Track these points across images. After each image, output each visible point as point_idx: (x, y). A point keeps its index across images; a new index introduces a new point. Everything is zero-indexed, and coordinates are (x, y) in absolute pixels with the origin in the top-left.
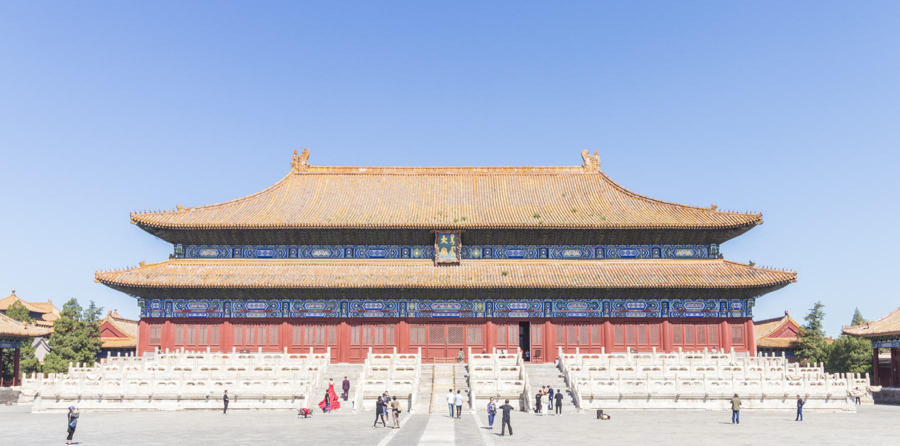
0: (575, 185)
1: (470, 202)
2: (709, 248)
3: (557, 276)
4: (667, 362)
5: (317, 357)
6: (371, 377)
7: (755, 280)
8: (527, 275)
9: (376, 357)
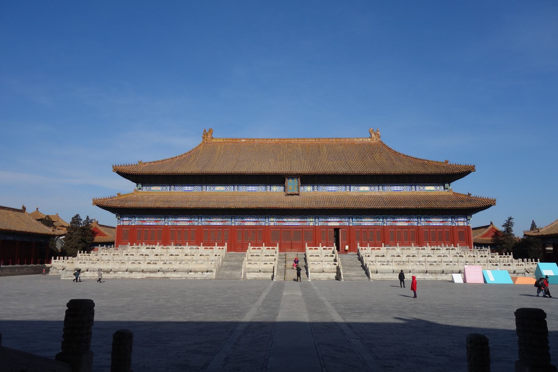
0: (366, 149)
1: (305, 159)
2: (444, 186)
3: (356, 202)
4: (420, 252)
5: (219, 248)
6: (250, 260)
7: (471, 204)
8: (339, 201)
9: (253, 249)
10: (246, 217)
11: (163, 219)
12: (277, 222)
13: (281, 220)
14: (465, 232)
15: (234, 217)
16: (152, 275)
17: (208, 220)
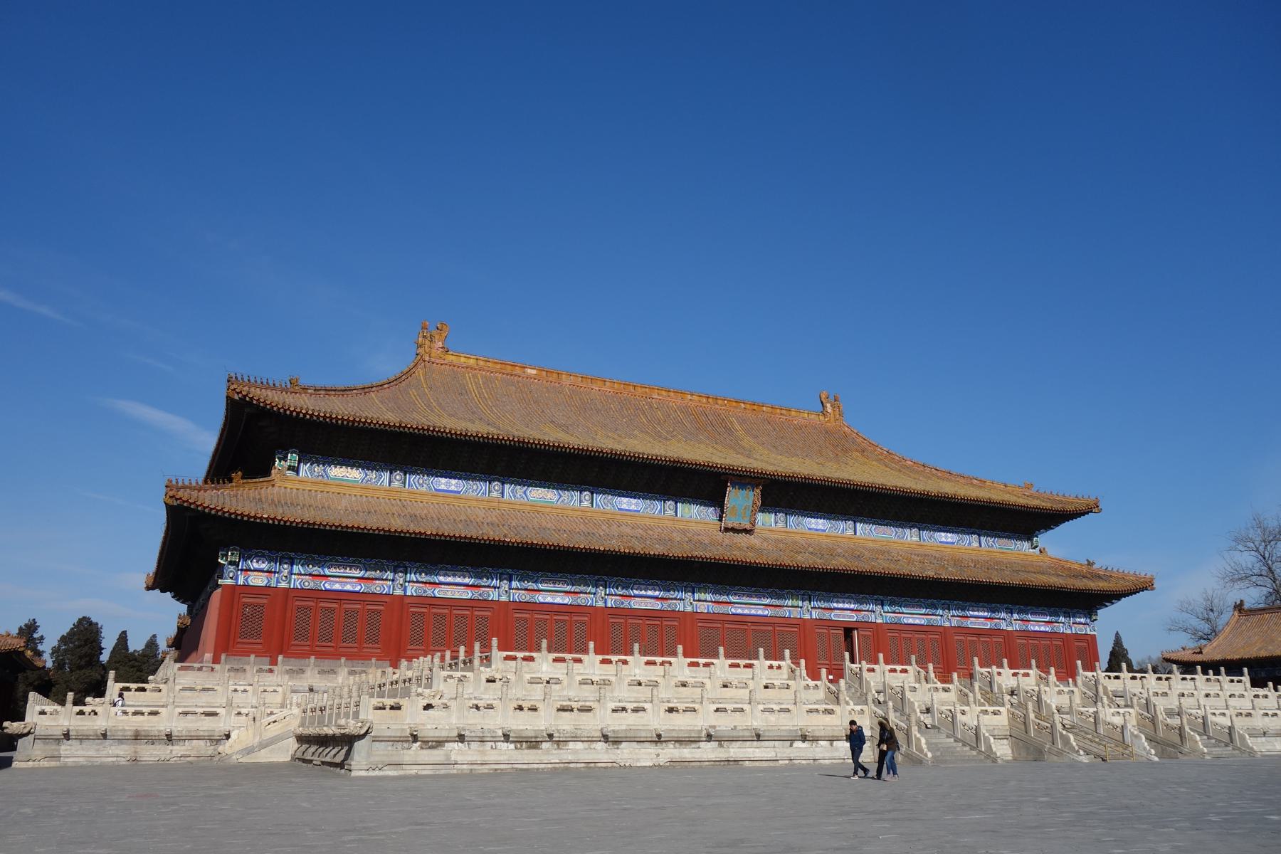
5: (771, 667)
10: (635, 583)
11: (390, 575)
12: (715, 602)
13: (724, 598)
14: (1087, 649)
15: (604, 580)
16: (687, 753)
17: (531, 585)
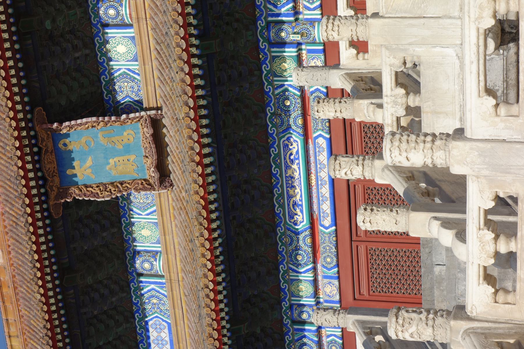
12: (315, 262)
